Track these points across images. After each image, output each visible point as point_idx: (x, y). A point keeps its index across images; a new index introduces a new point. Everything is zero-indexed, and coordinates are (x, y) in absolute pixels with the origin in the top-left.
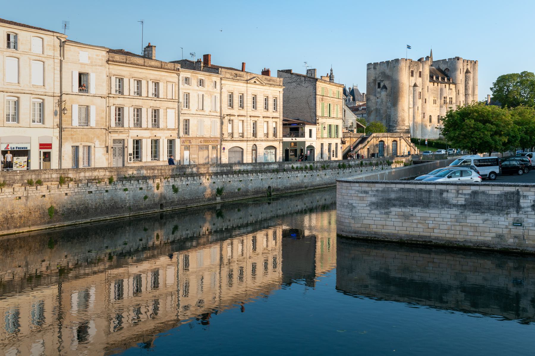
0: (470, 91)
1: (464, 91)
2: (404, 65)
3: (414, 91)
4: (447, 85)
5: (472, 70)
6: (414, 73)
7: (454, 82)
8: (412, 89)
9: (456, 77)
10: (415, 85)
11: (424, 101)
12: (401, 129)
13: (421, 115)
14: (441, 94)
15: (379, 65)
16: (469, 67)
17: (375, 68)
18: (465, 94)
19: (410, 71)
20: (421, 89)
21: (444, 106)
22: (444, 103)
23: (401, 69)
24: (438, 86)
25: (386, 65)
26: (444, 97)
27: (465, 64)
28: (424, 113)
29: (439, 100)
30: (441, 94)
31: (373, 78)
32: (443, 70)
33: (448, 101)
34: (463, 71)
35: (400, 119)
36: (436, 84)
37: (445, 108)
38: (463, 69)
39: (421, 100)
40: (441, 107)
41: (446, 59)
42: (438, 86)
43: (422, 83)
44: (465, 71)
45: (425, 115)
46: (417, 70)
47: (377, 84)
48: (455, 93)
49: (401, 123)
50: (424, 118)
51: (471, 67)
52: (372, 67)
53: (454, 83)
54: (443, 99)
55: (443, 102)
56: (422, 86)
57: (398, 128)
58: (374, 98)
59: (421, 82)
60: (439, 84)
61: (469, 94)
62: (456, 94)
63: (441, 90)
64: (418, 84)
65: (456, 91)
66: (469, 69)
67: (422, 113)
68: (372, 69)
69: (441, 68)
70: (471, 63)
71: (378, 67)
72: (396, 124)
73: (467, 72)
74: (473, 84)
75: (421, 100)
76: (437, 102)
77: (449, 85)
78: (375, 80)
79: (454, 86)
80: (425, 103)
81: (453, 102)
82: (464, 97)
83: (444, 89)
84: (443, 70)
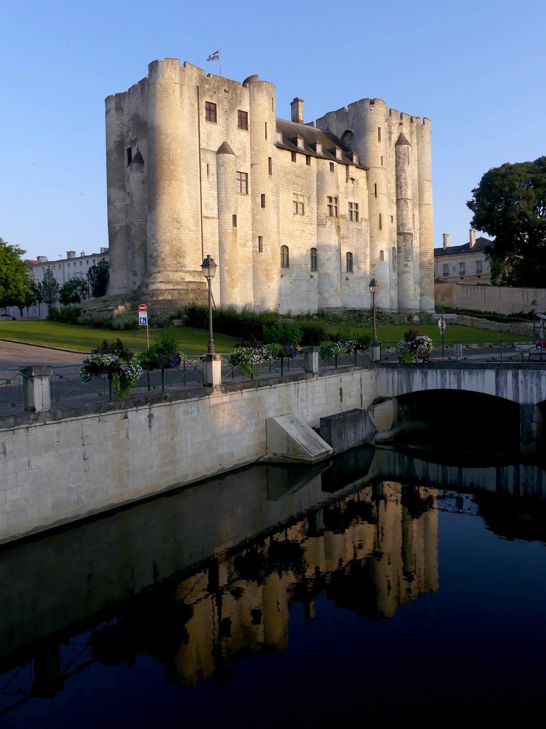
0: (409, 192)
1: (393, 190)
2: (177, 79)
3: (219, 166)
4: (340, 169)
5: (415, 141)
6: (219, 112)
7: (362, 163)
8: (211, 159)
9: (366, 150)
10: (224, 149)
11: (259, 201)
12: (169, 282)
13: (250, 244)
14: (320, 190)
15: (127, 97)
16: (406, 131)
17: (119, 109)
18: (398, 200)
19: (203, 105)
20: (249, 166)
21: (329, 223)
22: (331, 214)
23: (166, 90)
24: (308, 163)
25: (139, 90)
26: (330, 198)
27: (395, 120)
28: (260, 238)
29: (314, 205)
30: (320, 190)
31: (115, 138)
32: (339, 137)
33: (344, 210)
34: (390, 138)
35: (165, 250)
36: (301, 159)
37: (334, 230)
38: (390, 133)
39: (248, 200)
40: (320, 224)
41: (344, 108)
42: (308, 163)
43: (252, 149)
44: (395, 138)
45: (264, 242)
46: (232, 106)
47: (126, 153)
48: (366, 192)
49: (169, 261)
50: (260, 250)
51: (411, 133)
52: (112, 105)
53: (361, 166)
54: (326, 202)
55: (326, 210)
56: (252, 156)
57: (160, 277)
58: (121, 194)
59: (248, 146)
60: (313, 160)
61: (405, 200)
62: (370, 194)
63: (320, 176)
64: (233, 147)
65: (368, 188)
66: (407, 137)
67: (254, 237)
68: (113, 112)
69: (335, 132)
70: (412, 121)
71: (125, 105)
72: (155, 264)
73: (401, 141)
74: (419, 175)
75: (248, 200)
76: (306, 210)
77: (347, 169)
78: (120, 144)
79: (363, 173)
80: (263, 206)
81: (360, 217)
82: (395, 207)
83: (329, 176)
84: (339, 137)
